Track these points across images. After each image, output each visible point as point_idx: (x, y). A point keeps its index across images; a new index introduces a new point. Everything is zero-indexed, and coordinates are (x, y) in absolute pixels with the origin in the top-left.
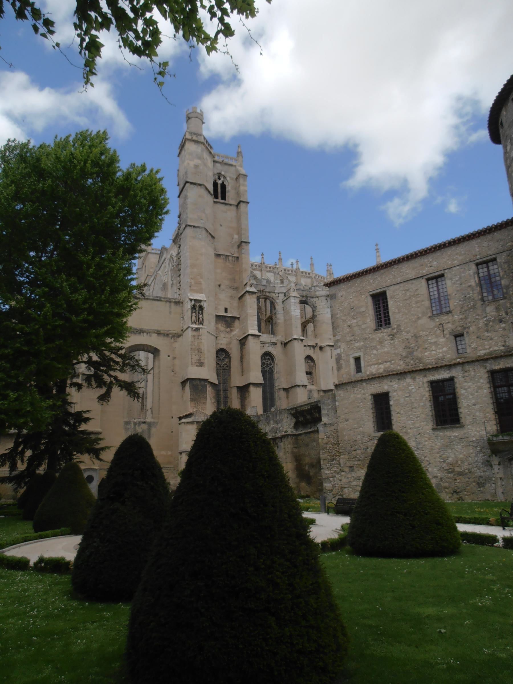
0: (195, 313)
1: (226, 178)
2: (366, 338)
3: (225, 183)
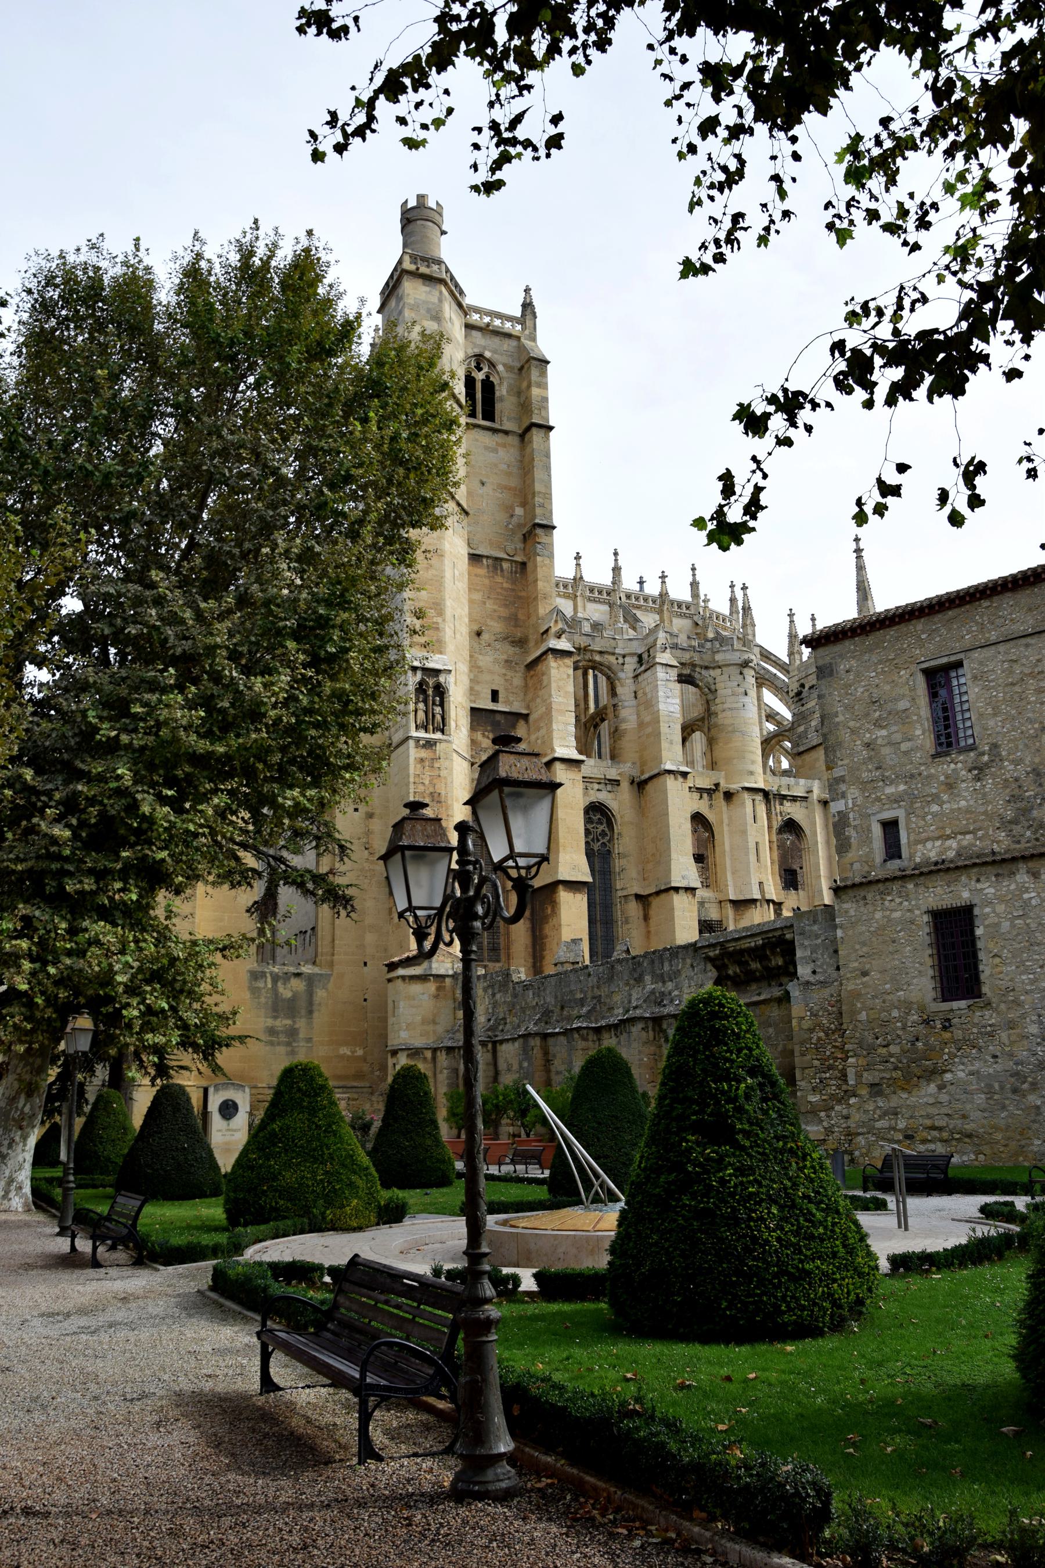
0: (425, 702)
2: (912, 776)
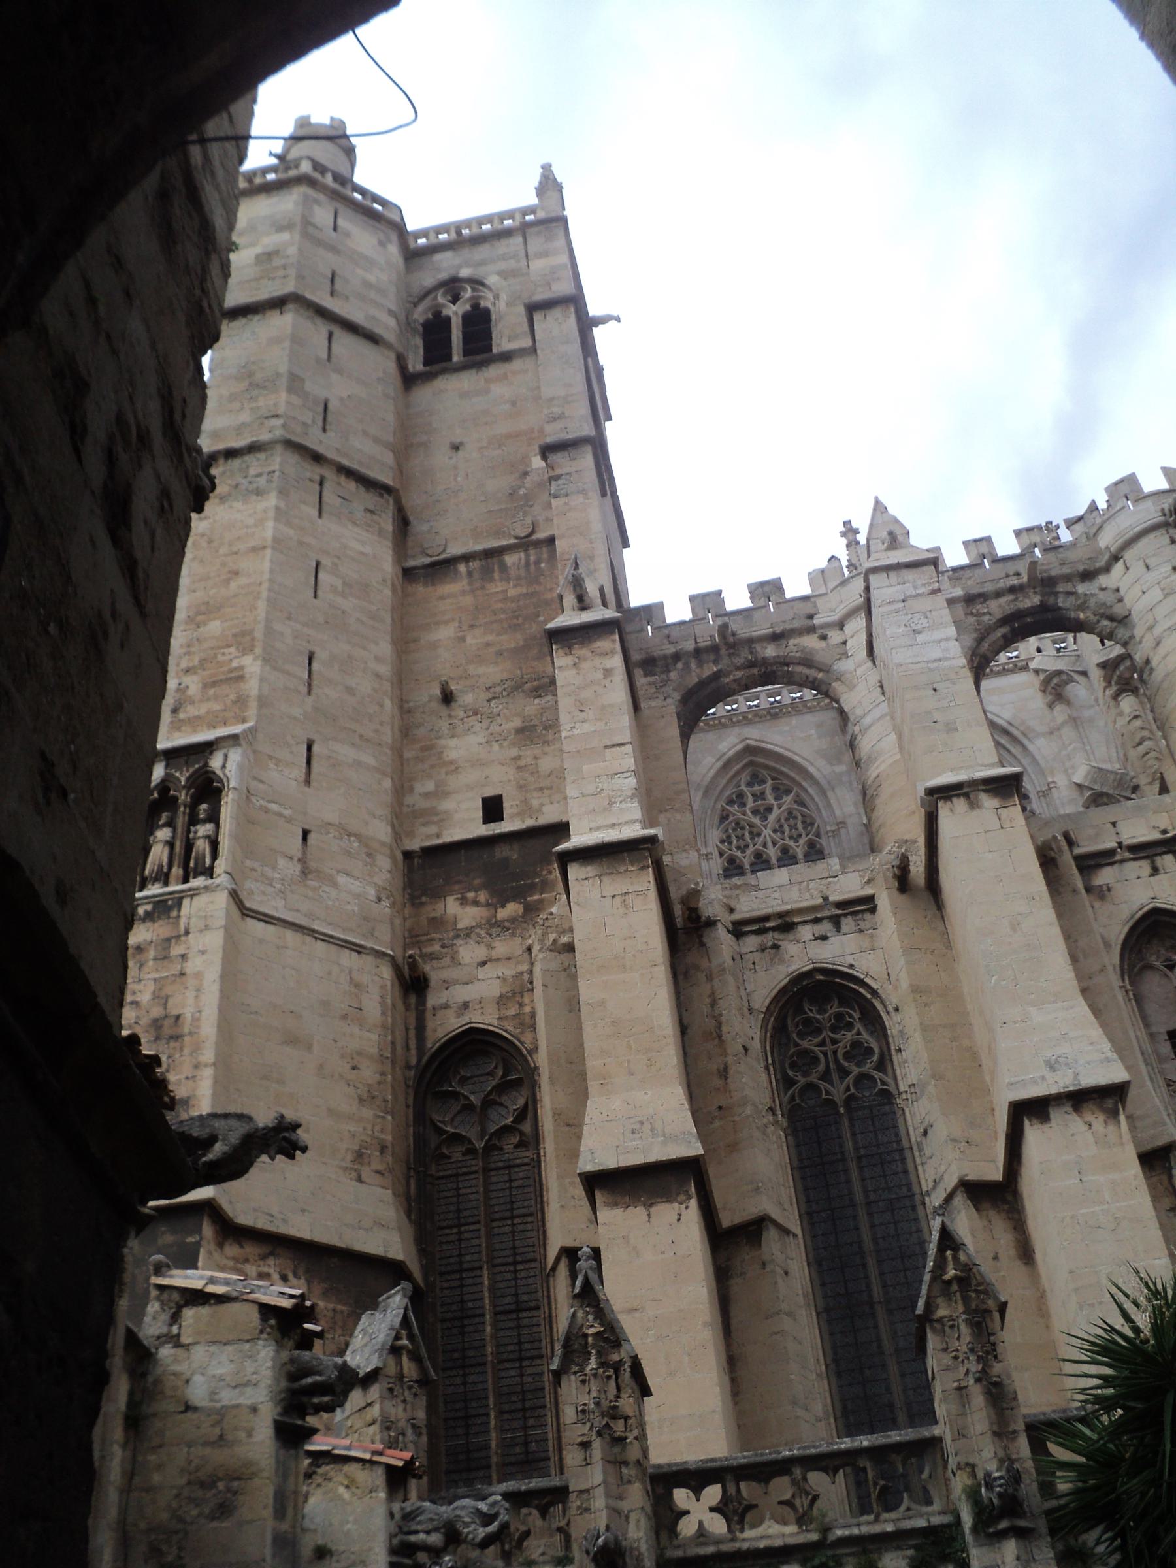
1: (483, 284)
3: (483, 304)
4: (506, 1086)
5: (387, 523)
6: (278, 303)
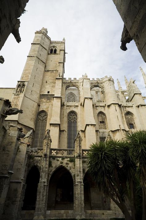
4: (45, 115)
5: (44, 66)
6: (38, 44)
